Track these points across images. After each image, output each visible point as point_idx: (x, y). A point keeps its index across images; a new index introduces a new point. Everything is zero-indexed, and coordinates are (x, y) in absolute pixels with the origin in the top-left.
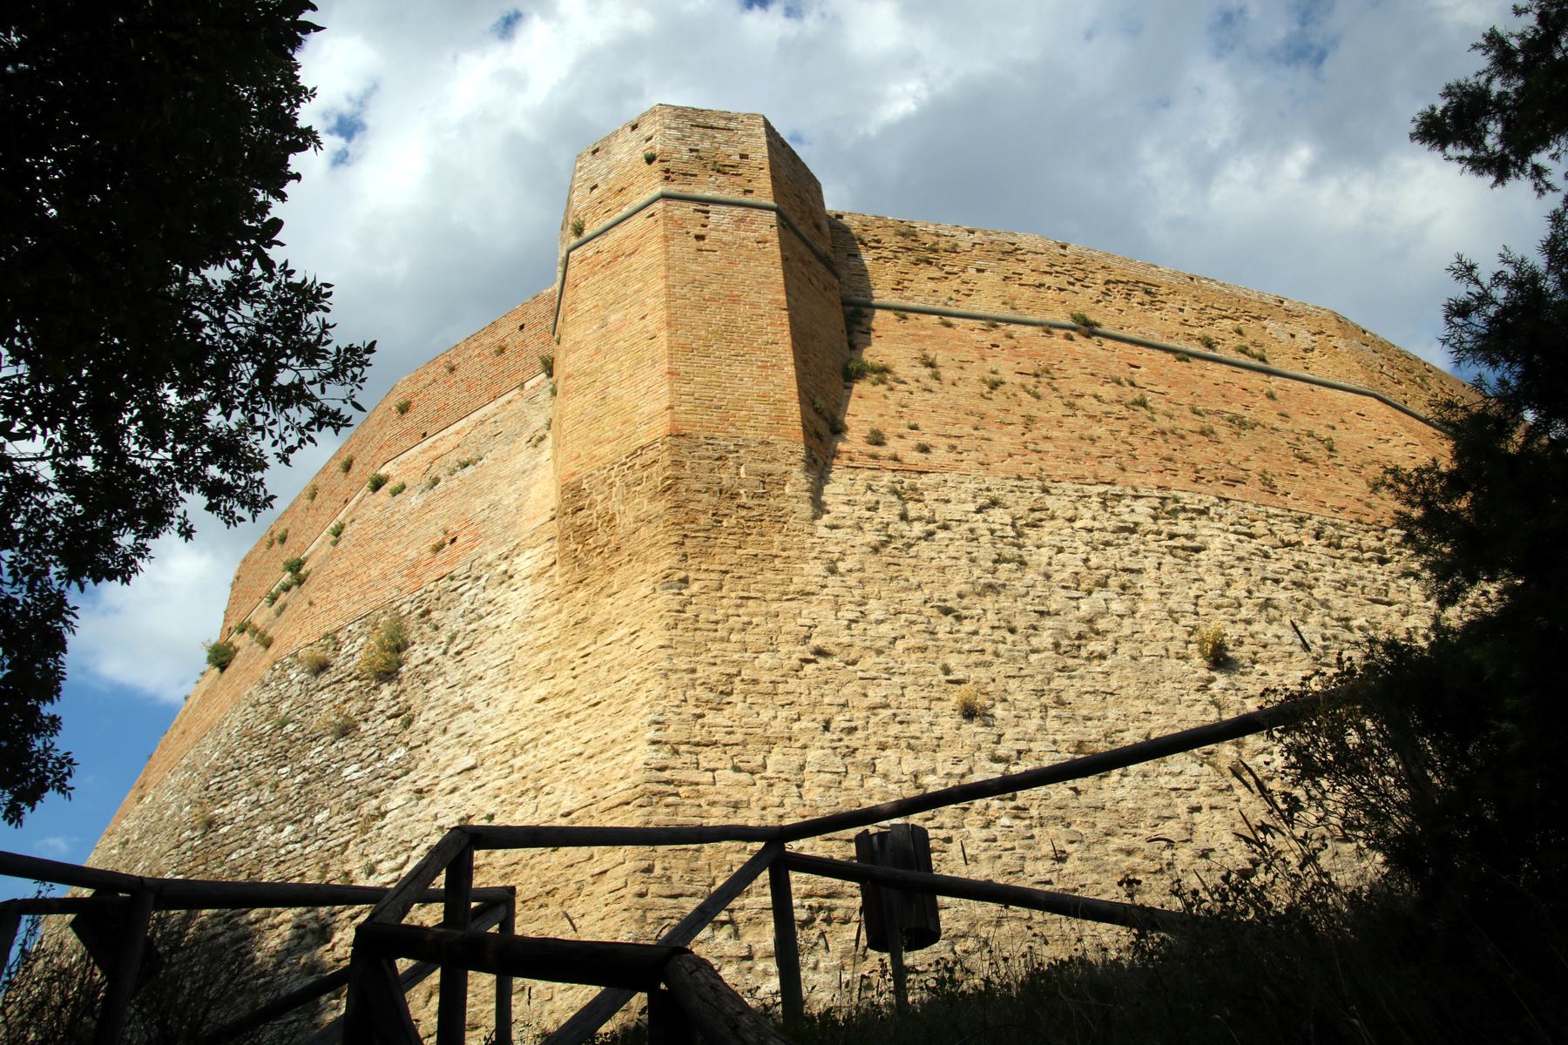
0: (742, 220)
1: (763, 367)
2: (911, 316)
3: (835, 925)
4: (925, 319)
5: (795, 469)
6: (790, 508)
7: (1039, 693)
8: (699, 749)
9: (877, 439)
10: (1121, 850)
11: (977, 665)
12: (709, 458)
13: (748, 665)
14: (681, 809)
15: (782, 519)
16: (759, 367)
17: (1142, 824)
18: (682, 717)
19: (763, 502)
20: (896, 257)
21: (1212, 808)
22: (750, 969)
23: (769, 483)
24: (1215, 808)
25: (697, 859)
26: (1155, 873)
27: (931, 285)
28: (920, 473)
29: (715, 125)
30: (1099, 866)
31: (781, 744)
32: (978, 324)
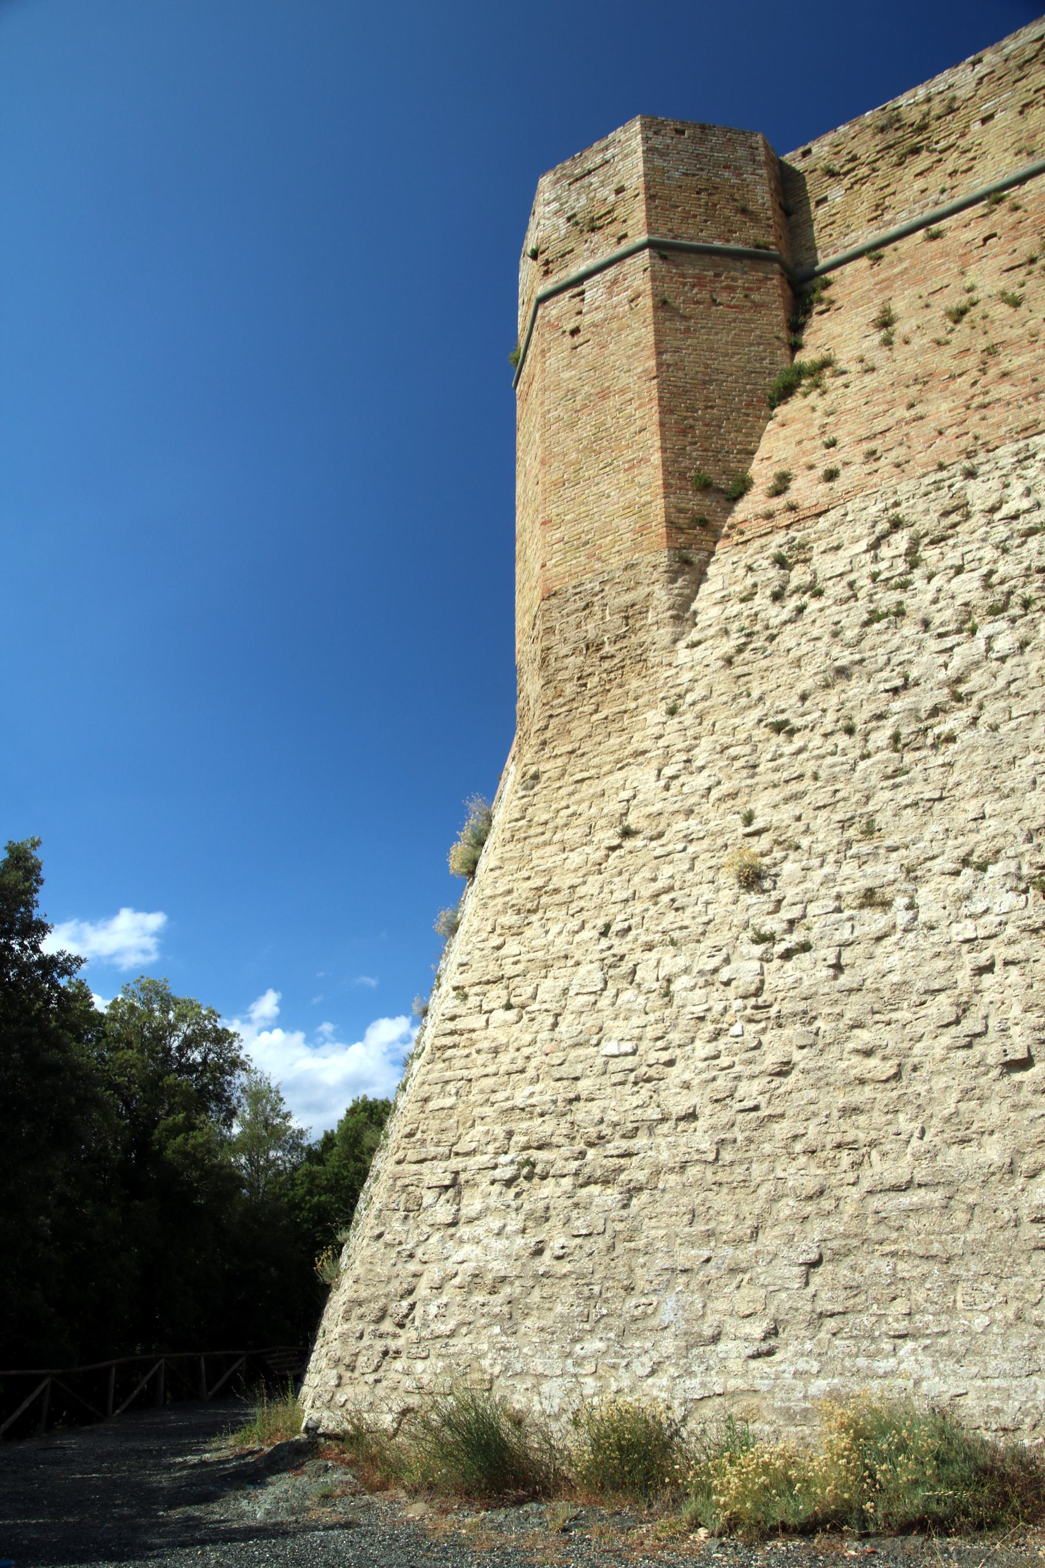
0: (615, 282)
1: (630, 468)
2: (887, 250)
3: (536, 1180)
4: (904, 245)
5: (657, 587)
6: (650, 640)
7: (845, 824)
8: (488, 987)
9: (781, 485)
10: (857, 1051)
11: (787, 800)
12: (577, 610)
13: (558, 871)
14: (454, 1061)
15: (643, 657)
16: (626, 470)
17: (905, 1005)
18: (484, 952)
19: (625, 643)
20: (874, 170)
21: (1007, 963)
22: (452, 1236)
23: (630, 614)
24: (1013, 963)
25: (451, 1117)
26: (887, 1081)
27: (920, 184)
28: (819, 515)
29: (592, 166)
30: (819, 1079)
31: (557, 964)
32: (979, 209)
